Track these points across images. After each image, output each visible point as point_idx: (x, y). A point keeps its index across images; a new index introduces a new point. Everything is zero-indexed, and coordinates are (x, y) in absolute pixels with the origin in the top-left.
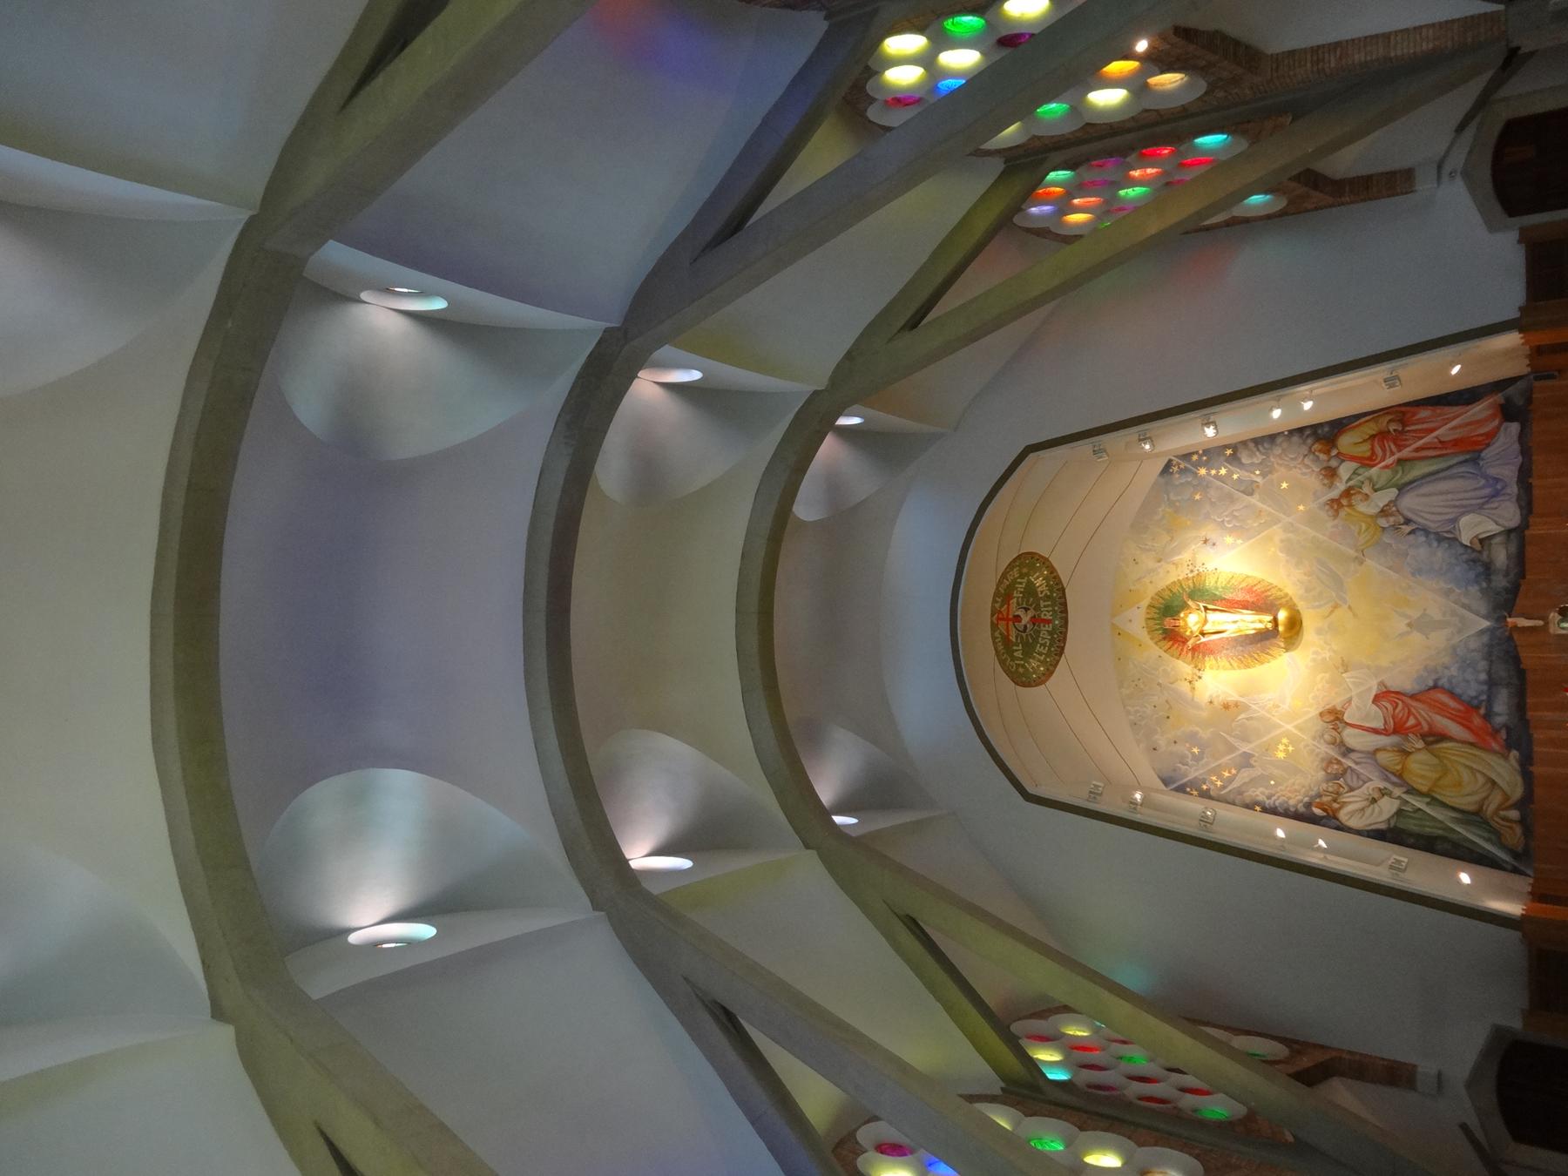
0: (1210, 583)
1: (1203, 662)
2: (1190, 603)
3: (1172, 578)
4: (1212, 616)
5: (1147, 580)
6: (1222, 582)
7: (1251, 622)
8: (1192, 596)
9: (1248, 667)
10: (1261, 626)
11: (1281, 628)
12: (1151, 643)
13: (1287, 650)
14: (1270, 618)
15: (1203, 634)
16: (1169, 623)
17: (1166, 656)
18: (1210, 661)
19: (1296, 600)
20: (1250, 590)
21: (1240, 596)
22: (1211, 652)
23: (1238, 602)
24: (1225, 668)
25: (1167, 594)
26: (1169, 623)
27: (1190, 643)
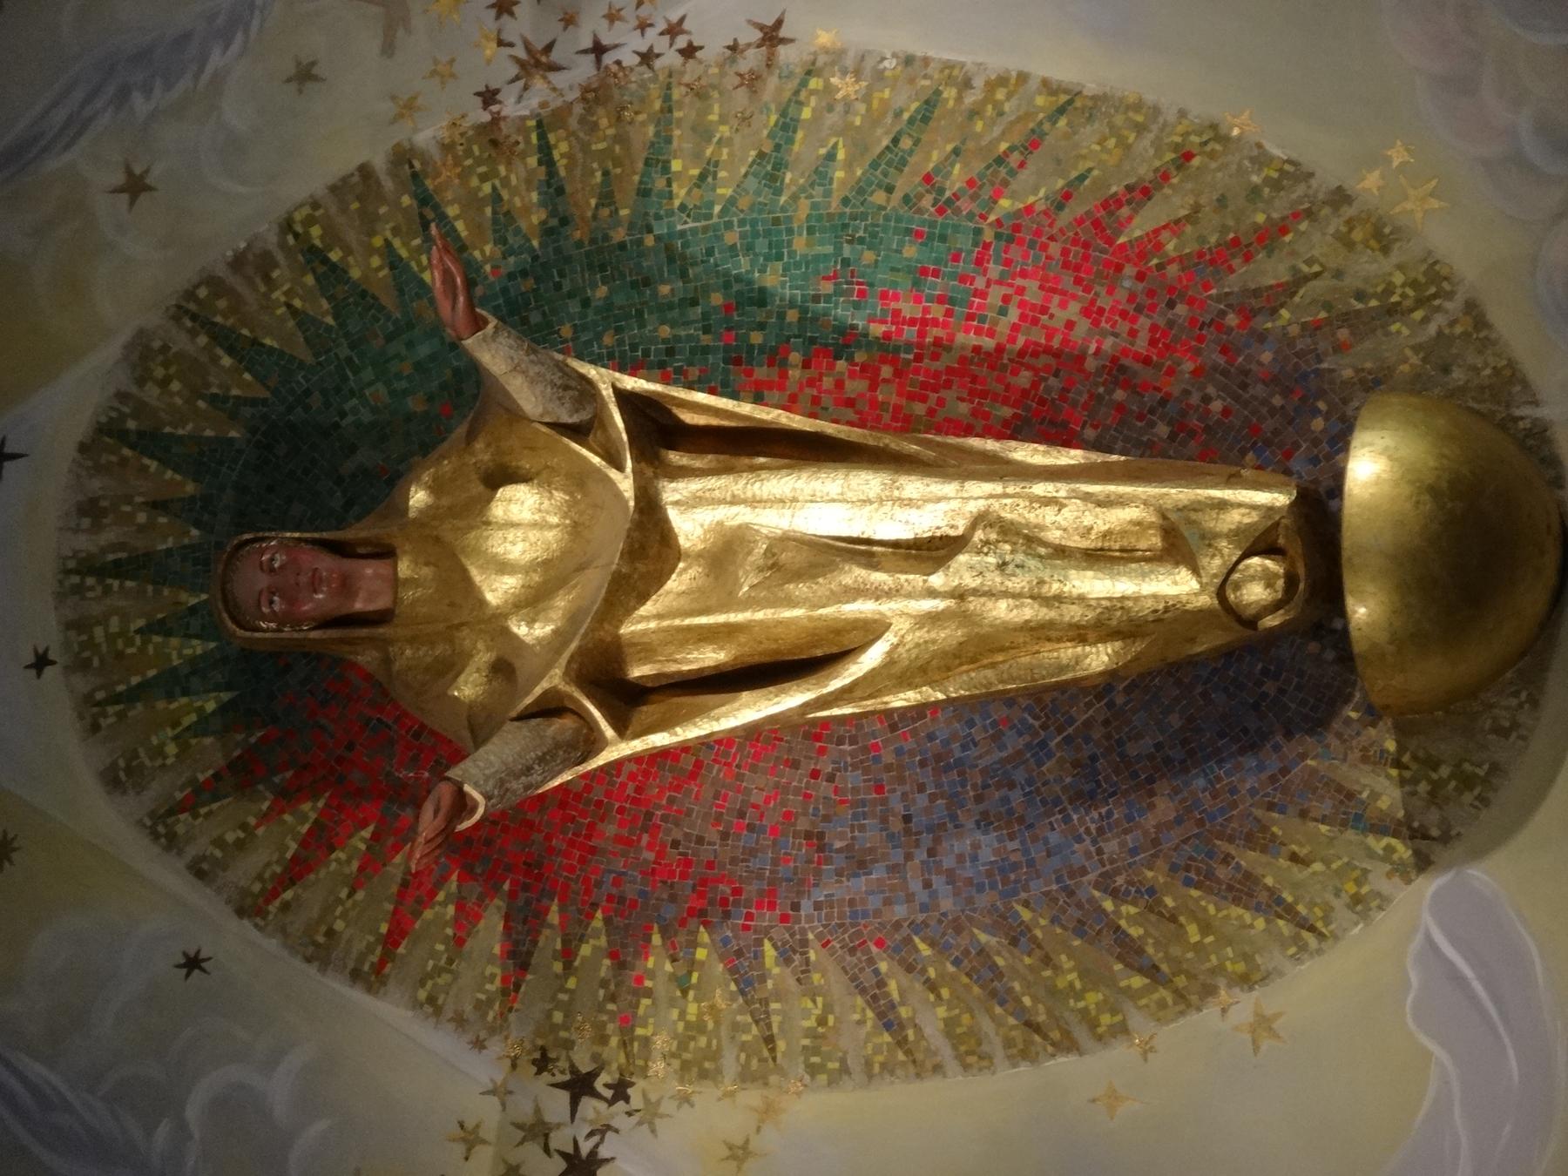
0: (708, 178)
1: (624, 987)
2: (495, 354)
3: (344, 138)
4: (698, 509)
5: (94, 165)
6: (830, 160)
7: (1078, 551)
8: (531, 311)
9: (1041, 1035)
10: (1177, 586)
11: (1363, 610)
12: (110, 822)
13: (1427, 843)
14: (1259, 499)
15: (628, 700)
16: (285, 585)
17: (239, 945)
18: (683, 994)
19: (1516, 331)
20: (1092, 240)
21: (997, 314)
22: (705, 897)
23: (976, 372)
24: (825, 1065)
25: (284, 306)
26: (285, 585)
27: (481, 777)
